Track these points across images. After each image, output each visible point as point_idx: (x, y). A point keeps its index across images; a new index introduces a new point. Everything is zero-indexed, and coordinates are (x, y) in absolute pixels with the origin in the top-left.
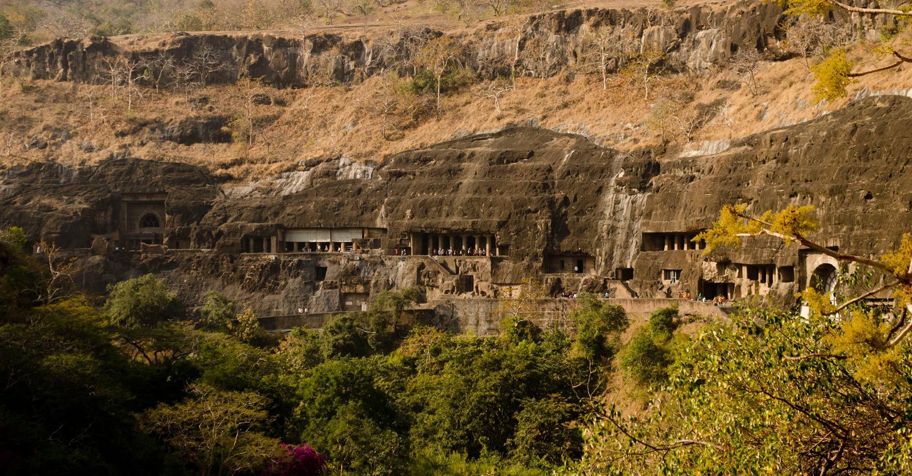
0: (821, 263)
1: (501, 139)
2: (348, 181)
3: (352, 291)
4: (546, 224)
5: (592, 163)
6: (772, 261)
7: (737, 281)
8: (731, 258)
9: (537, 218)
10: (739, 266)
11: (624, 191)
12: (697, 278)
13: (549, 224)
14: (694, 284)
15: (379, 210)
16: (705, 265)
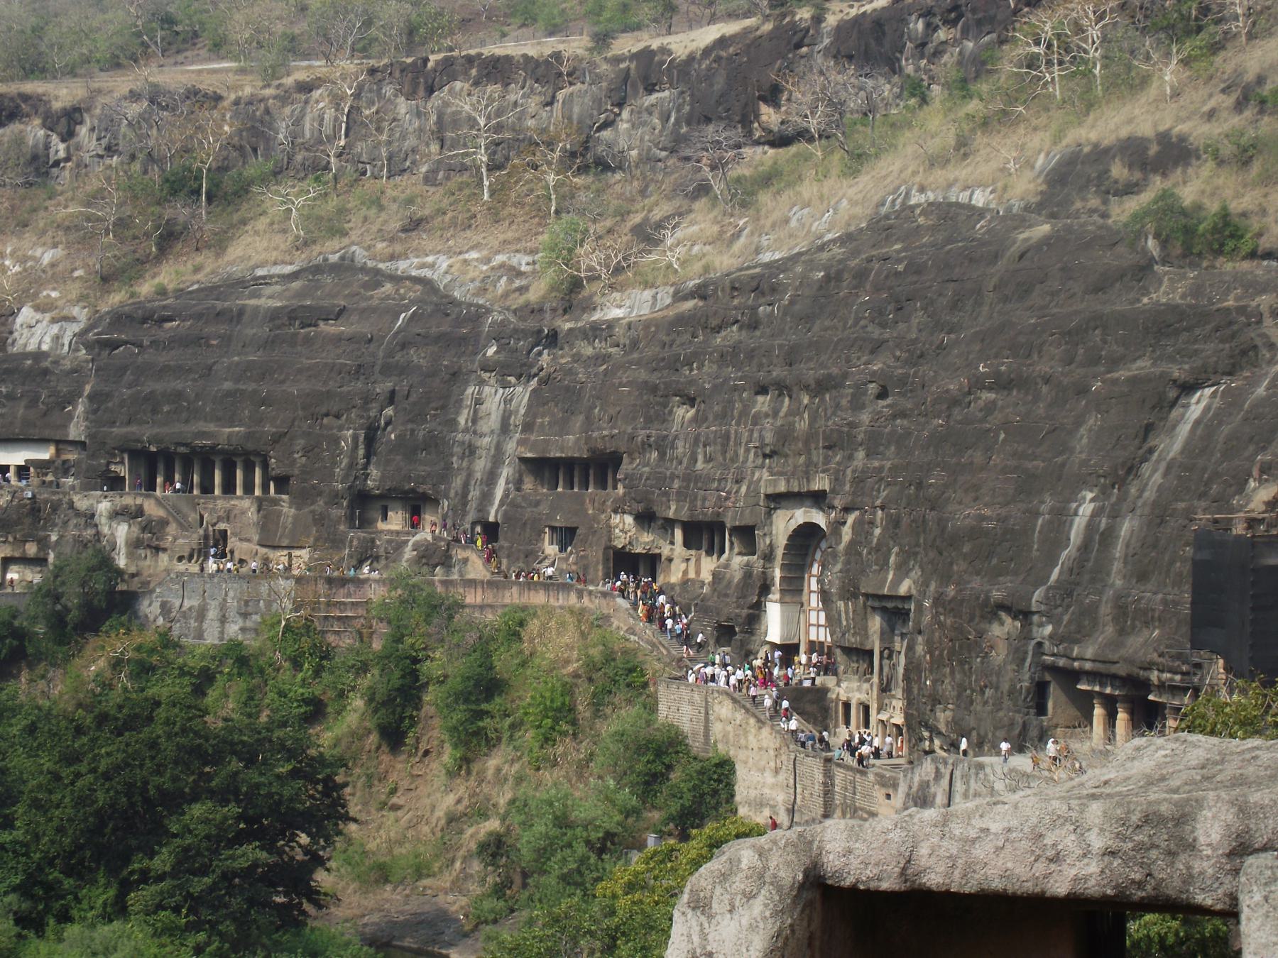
0: (801, 522)
1: (296, 285)
2: (26, 355)
3: (17, 555)
4: (355, 438)
5: (450, 331)
6: (718, 514)
7: (665, 551)
8: (655, 508)
9: (341, 428)
10: (669, 524)
11: (493, 381)
12: (603, 542)
13: (361, 439)
14: (595, 554)
15: (75, 408)
16: (616, 519)
